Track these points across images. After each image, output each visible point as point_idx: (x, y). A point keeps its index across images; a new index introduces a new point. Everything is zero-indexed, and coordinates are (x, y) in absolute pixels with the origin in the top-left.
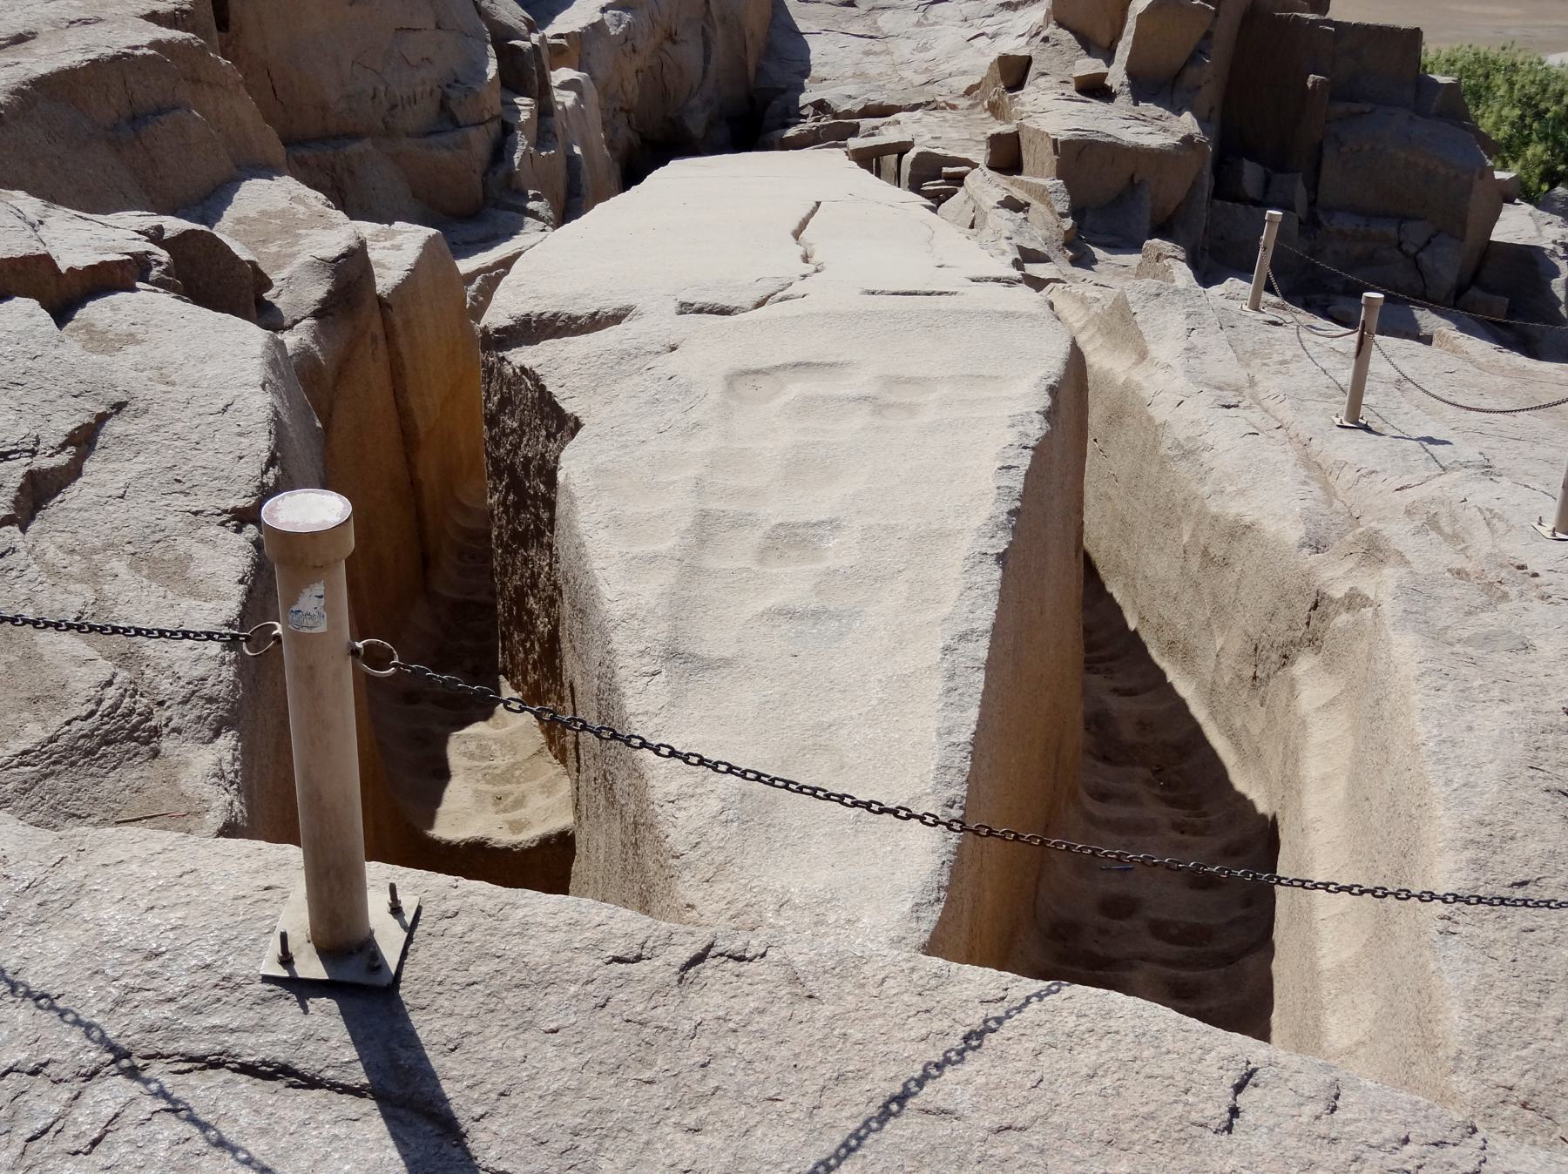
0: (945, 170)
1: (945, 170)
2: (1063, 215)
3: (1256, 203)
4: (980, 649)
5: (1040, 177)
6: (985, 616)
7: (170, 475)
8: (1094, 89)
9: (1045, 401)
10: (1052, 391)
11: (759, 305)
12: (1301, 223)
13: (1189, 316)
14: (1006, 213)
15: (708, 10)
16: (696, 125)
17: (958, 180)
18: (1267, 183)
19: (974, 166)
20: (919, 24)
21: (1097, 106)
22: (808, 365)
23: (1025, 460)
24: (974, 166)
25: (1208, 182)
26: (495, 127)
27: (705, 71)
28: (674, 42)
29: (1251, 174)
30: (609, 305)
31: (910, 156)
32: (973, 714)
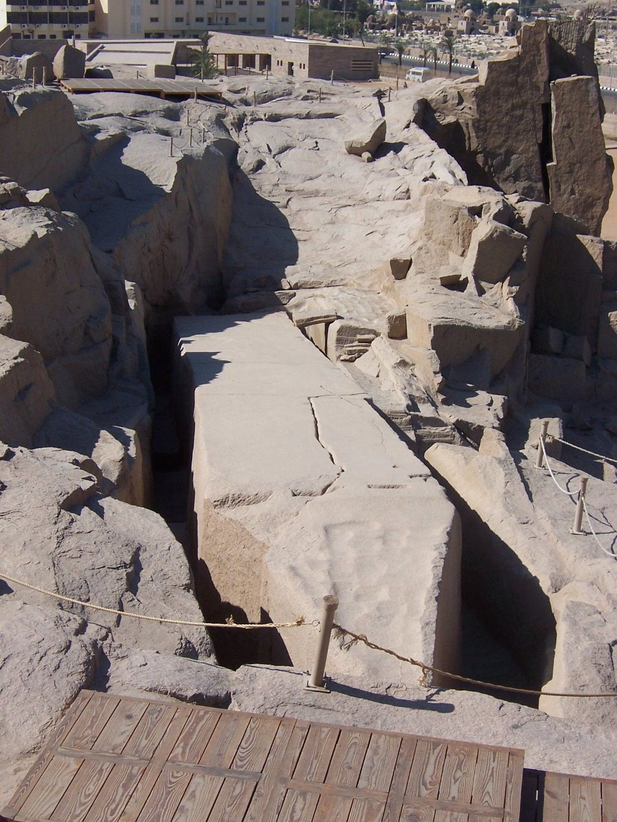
0: (359, 337)
1: (359, 337)
2: (435, 373)
3: (557, 355)
4: (433, 626)
5: (419, 345)
6: (433, 617)
7: (162, 573)
8: (454, 284)
9: (445, 538)
10: (448, 533)
11: (324, 491)
12: (587, 367)
13: (506, 475)
14: (401, 371)
15: (192, 217)
16: (186, 294)
17: (369, 342)
18: (565, 341)
19: (377, 334)
20: (332, 223)
21: (456, 295)
22: (354, 522)
23: (442, 563)
24: (377, 334)
25: (526, 346)
26: (110, 341)
27: (189, 257)
28: (171, 240)
29: (554, 337)
30: (263, 491)
31: (335, 326)
32: (433, 646)
